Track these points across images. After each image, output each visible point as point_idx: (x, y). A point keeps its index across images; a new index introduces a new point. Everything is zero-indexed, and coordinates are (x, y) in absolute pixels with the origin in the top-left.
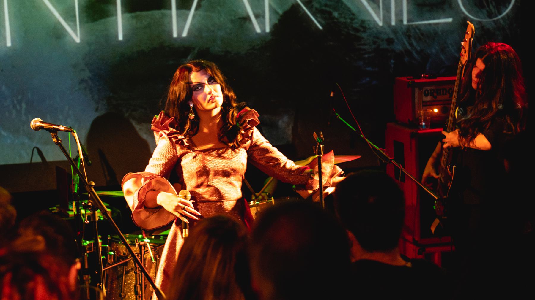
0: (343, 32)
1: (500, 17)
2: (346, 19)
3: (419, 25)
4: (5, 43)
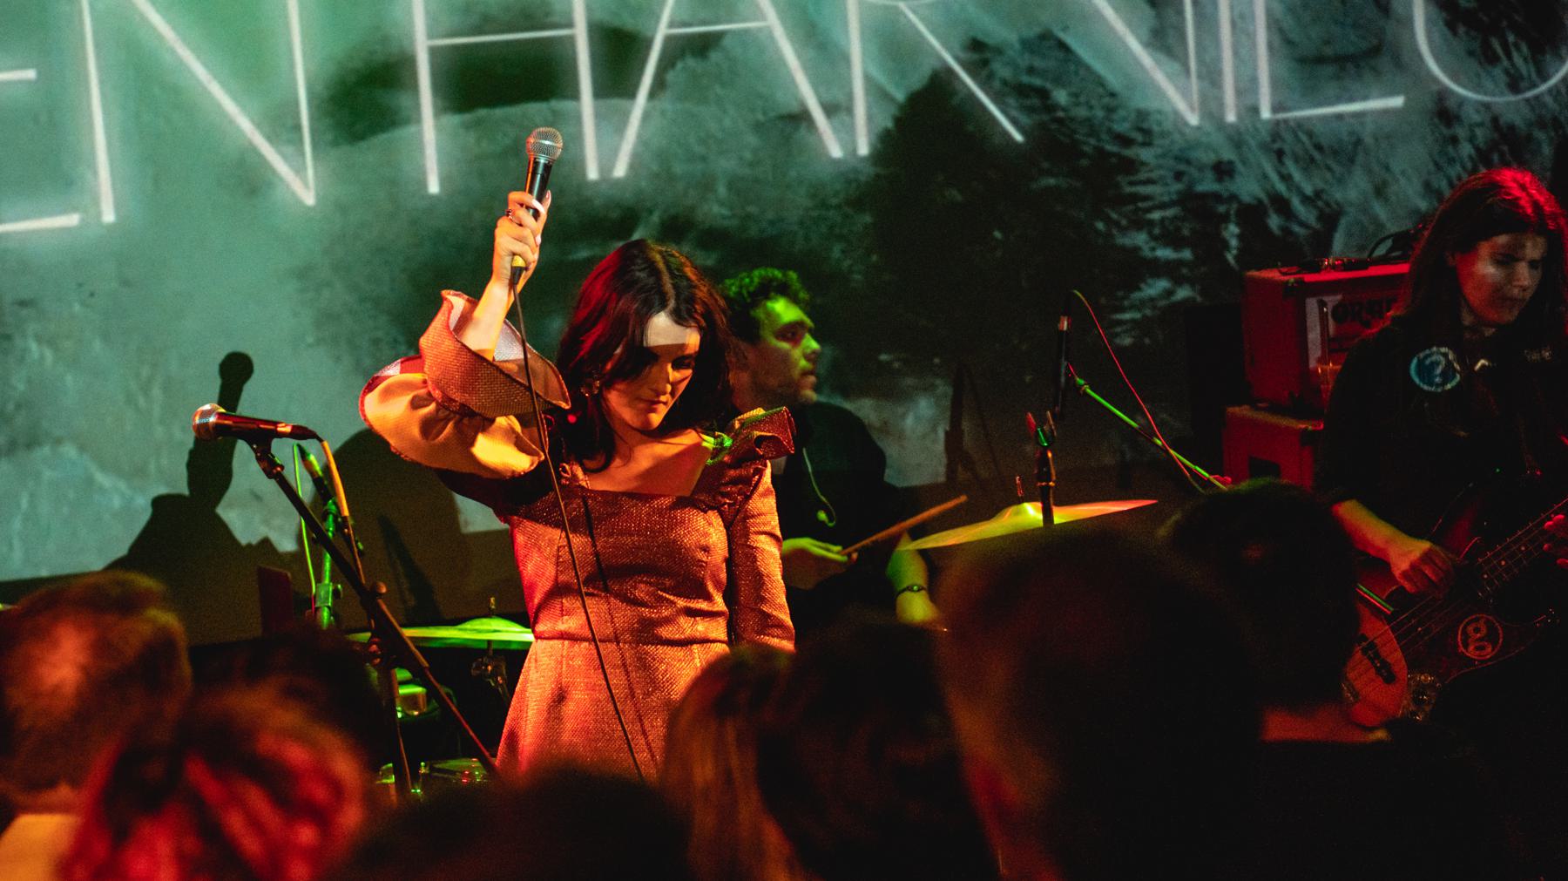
0: (1086, 148)
1: (1544, 87)
3: (1309, 119)
4: (99, 214)
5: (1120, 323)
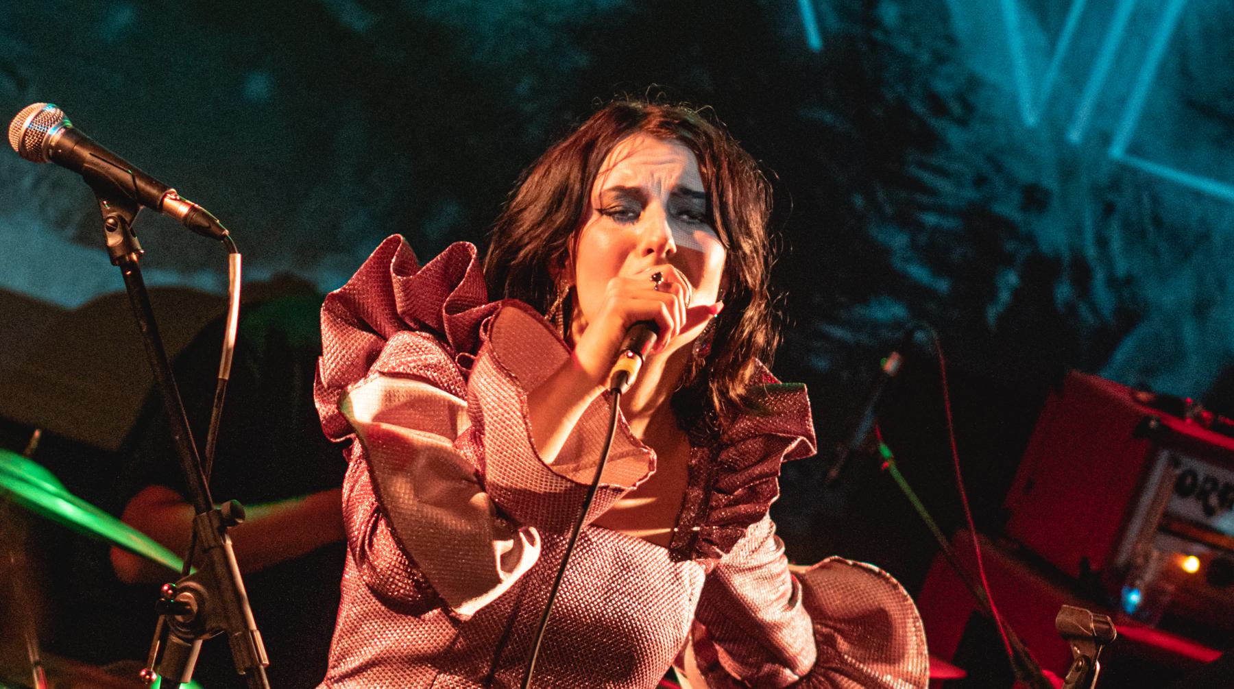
0: (889, 96)
2: (918, 45)
3: (1161, 181)
5: (826, 337)
